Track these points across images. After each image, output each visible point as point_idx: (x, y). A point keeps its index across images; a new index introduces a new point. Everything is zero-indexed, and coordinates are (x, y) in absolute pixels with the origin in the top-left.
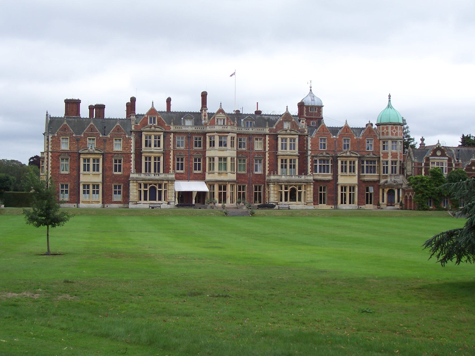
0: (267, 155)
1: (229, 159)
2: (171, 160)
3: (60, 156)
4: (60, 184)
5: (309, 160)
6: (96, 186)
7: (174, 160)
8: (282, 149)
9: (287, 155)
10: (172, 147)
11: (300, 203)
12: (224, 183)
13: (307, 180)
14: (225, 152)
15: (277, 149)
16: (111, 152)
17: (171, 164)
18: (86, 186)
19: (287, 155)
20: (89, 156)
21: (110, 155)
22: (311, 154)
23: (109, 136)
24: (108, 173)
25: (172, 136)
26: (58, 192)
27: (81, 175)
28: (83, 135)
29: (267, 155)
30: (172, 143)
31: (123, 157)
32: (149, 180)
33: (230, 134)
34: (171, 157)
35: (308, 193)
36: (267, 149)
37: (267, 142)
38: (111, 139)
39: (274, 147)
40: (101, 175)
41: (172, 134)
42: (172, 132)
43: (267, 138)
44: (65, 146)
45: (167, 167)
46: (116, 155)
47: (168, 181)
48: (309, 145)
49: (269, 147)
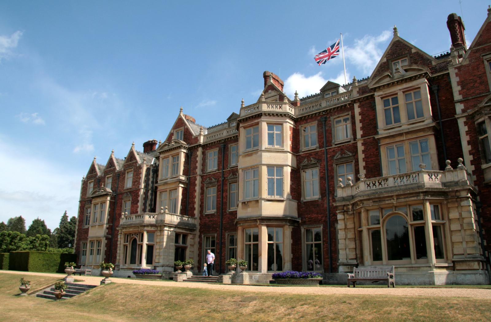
0: (360, 148)
2: (197, 194)
4: (81, 243)
5: (463, 129)
8: (388, 122)
9: (401, 135)
10: (198, 171)
15: (376, 127)
18: (92, 242)
19: (401, 135)
22: (464, 111)
26: (79, 254)
29: (360, 148)
30: (199, 165)
33: (263, 118)
34: (198, 188)
35: (455, 226)
36: (359, 133)
37: (358, 118)
38: (124, 174)
39: (370, 125)
41: (200, 149)
42: (200, 145)
43: (357, 110)
46: (125, 195)
48: (456, 89)
49: (362, 128)
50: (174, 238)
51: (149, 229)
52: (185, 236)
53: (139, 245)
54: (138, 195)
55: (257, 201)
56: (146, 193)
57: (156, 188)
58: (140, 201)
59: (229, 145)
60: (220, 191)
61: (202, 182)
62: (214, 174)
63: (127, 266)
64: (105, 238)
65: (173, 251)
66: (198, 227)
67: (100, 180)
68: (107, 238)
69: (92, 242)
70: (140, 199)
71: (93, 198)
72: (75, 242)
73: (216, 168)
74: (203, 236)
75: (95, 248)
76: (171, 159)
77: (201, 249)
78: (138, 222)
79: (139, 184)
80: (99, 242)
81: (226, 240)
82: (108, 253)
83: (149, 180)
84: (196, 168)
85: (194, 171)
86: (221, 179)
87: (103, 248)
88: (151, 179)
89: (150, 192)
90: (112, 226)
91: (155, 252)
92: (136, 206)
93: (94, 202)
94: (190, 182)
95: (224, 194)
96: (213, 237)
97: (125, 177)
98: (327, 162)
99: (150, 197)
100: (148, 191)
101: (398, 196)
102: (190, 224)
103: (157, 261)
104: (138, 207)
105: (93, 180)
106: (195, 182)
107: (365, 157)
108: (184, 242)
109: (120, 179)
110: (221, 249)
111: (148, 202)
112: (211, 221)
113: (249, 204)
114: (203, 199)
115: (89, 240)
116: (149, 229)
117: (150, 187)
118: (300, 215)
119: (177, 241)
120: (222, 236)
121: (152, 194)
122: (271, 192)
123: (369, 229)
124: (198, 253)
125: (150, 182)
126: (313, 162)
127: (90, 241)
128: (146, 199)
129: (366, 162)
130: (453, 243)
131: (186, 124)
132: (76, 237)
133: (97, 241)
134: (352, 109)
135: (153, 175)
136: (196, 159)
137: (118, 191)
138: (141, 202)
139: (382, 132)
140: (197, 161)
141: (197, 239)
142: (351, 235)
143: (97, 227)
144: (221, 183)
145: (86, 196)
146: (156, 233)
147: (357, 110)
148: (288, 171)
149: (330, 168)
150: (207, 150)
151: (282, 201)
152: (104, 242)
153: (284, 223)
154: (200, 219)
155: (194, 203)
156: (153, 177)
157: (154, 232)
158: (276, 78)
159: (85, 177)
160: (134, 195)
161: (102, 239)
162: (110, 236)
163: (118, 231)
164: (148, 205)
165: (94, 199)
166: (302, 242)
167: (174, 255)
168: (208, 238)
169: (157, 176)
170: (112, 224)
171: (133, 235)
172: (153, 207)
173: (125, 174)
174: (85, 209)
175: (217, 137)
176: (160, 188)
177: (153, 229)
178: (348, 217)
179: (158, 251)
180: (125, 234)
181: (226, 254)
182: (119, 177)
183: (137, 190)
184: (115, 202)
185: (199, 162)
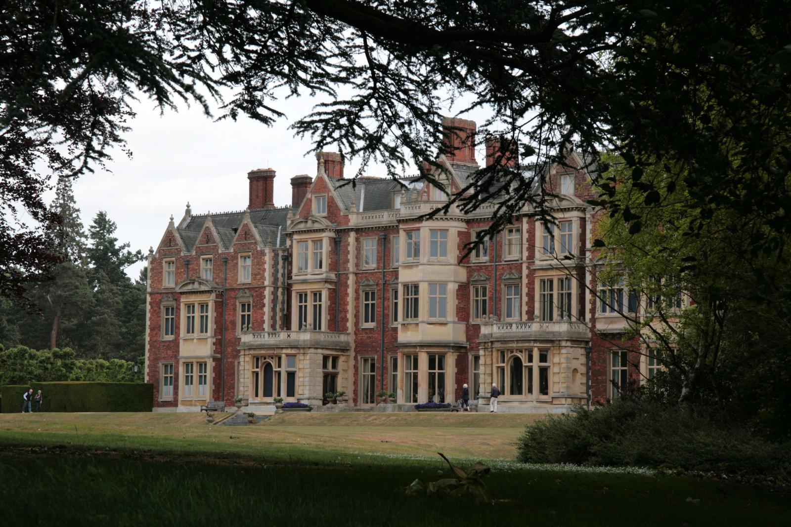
1: (423, 288)
2: (350, 299)
3: (160, 301)
4: (160, 364)
6: (202, 365)
7: (357, 298)
11: (530, 397)
12: (412, 350)
13: (553, 333)
14: (414, 269)
16: (235, 286)
17: (350, 308)
18: (188, 366)
20: (193, 299)
21: (232, 294)
22: (591, 260)
23: (232, 251)
24: (229, 336)
25: (352, 238)
26: (158, 383)
27: (181, 341)
28: (194, 253)
30: (351, 257)
31: (253, 296)
32: (261, 347)
34: (351, 291)
35: (556, 370)
36: (526, 254)
38: (235, 258)
40: (210, 341)
41: (353, 235)
42: (352, 230)
44: (169, 282)
45: (342, 314)
46: (241, 294)
47: (297, 348)
50: (322, 362)
51: (289, 351)
52: (335, 359)
53: (276, 371)
55: (417, 324)
56: (274, 294)
57: (290, 285)
58: (267, 305)
59: (391, 236)
60: (380, 298)
61: (357, 282)
62: (372, 274)
63: (258, 400)
64: (211, 359)
65: (320, 380)
66: (353, 345)
67: (188, 261)
68: (215, 359)
69: (188, 366)
70: (266, 301)
71: (181, 293)
72: (147, 363)
73: (374, 266)
74: (359, 357)
75: (195, 374)
76: (310, 244)
77: (357, 374)
78: (272, 342)
79: (263, 278)
80: (202, 365)
81: (389, 365)
82: (218, 381)
83: (278, 272)
84: (348, 261)
85: (345, 266)
86: (381, 282)
87: (210, 374)
88: (281, 271)
89: (280, 290)
90: (221, 340)
91: (298, 381)
92: (261, 311)
93: (184, 300)
94: (339, 280)
95: (385, 303)
96: (373, 359)
97: (237, 263)
98: (496, 280)
99: (280, 298)
100: (278, 288)
101: (518, 341)
102: (342, 342)
103: (300, 392)
104: (264, 314)
105: (173, 259)
106: (346, 283)
107: (528, 283)
108: (334, 366)
109: (229, 266)
110: (383, 376)
111: (279, 306)
112: (370, 338)
113: (409, 326)
114: (359, 306)
115: (181, 362)
116: (289, 351)
117: (280, 284)
118: (468, 339)
119: (325, 366)
120: (383, 359)
121: (283, 294)
122: (432, 314)
123: (498, 367)
124: (353, 380)
125: (280, 275)
126: (482, 279)
127: (184, 363)
128: (274, 301)
129: (529, 288)
130: (554, 383)
131: (329, 191)
132: (147, 354)
133: (197, 362)
134: (522, 221)
135: (284, 263)
136: (347, 248)
137: (227, 285)
138: (269, 307)
139: (538, 263)
140: (349, 251)
141: (352, 362)
142: (488, 371)
143: (195, 340)
144: (382, 287)
145: (161, 285)
146: (298, 356)
147: (525, 227)
148: (452, 287)
149: (498, 288)
150: (362, 236)
151: (444, 324)
153: (446, 350)
154: (356, 334)
155: (346, 311)
156: (284, 267)
157: (294, 355)
158: (461, 126)
159: (155, 249)
160: (257, 296)
161: (207, 360)
162: (219, 356)
163: (239, 351)
164: (278, 310)
165: (183, 296)
166: (470, 370)
167: (321, 385)
168: (366, 360)
169: (291, 263)
170: (220, 337)
171: (265, 359)
172: (285, 312)
173: (237, 258)
174: (162, 307)
175: (375, 220)
176: (295, 288)
177: (293, 351)
178: (487, 353)
179: (301, 379)
180: (254, 357)
181: (389, 383)
182: (226, 262)
183: (260, 288)
184: (222, 302)
185: (351, 253)
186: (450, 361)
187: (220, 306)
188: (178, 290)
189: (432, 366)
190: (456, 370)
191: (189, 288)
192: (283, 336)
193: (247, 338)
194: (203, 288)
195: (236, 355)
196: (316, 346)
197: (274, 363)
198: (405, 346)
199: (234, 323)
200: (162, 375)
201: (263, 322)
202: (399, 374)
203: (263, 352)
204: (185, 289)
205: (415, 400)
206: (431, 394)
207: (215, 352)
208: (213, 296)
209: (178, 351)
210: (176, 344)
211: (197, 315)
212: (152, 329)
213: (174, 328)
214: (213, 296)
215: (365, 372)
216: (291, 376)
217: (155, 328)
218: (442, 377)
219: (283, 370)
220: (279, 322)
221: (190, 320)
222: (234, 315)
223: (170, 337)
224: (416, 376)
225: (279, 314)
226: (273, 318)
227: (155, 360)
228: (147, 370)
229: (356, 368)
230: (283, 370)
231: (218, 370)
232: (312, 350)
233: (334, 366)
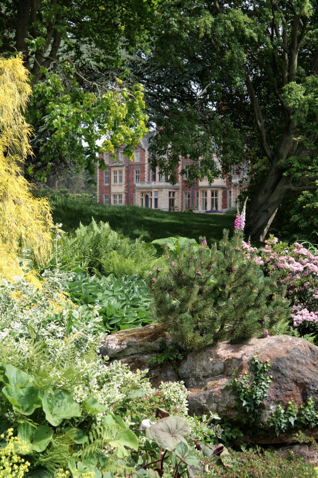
18: (115, 196)
20: (116, 169)
21: (132, 167)
24: (131, 184)
27: (112, 187)
32: (144, 188)
46: (135, 166)
51: (155, 190)
52: (174, 193)
54: (144, 168)
65: (168, 201)
66: (181, 187)
68: (125, 193)
69: (115, 196)
79: (144, 160)
80: (120, 196)
91: (159, 202)
93: (112, 169)
108: (173, 196)
115: (112, 194)
116: (155, 190)
119: (170, 196)
120: (193, 193)
141: (180, 194)
152: (124, 196)
157: (157, 192)
163: (135, 190)
168: (186, 193)
177: (157, 190)
186: (220, 193)
187: (127, 172)
188: (110, 165)
189: (212, 195)
190: (222, 197)
191: (115, 164)
192: (153, 184)
193: (138, 185)
194: (120, 164)
195: (134, 191)
196: (166, 188)
197: (149, 195)
198: (202, 187)
199: (133, 179)
200: (104, 200)
201: (145, 178)
202: (199, 199)
203: (145, 190)
204: (113, 165)
205: (206, 209)
206: (212, 207)
207: (126, 190)
208: (124, 168)
209: (110, 190)
210: (109, 188)
211: (118, 175)
212: (100, 181)
213: (109, 181)
214: (124, 168)
215: (186, 198)
216: (156, 200)
217: (101, 181)
218: (216, 199)
219: (153, 197)
220: (151, 178)
221: (115, 178)
222: (133, 175)
223: (107, 185)
224: (206, 200)
225: (151, 175)
226: (149, 176)
227: (101, 194)
228: (98, 198)
229: (182, 196)
230: (153, 197)
231: (127, 198)
232: (164, 190)
233: (173, 196)
